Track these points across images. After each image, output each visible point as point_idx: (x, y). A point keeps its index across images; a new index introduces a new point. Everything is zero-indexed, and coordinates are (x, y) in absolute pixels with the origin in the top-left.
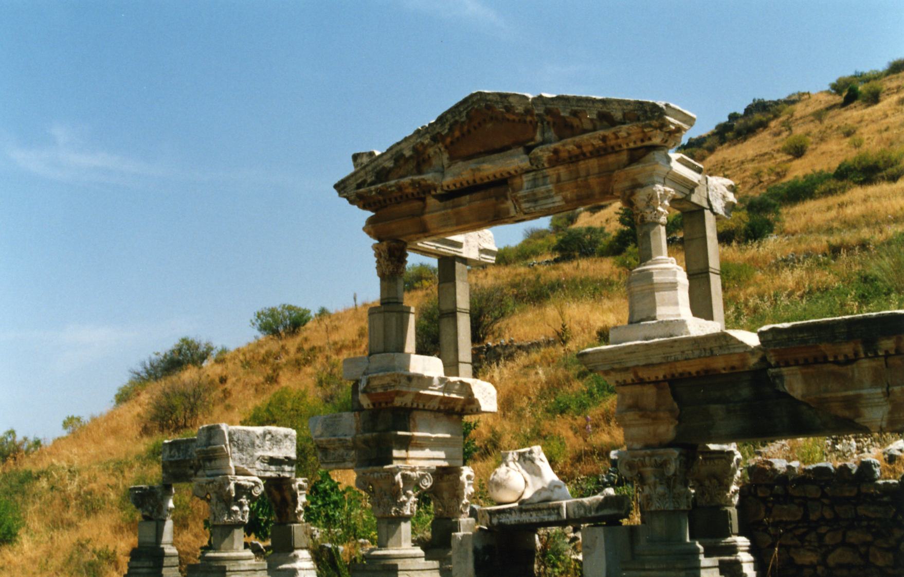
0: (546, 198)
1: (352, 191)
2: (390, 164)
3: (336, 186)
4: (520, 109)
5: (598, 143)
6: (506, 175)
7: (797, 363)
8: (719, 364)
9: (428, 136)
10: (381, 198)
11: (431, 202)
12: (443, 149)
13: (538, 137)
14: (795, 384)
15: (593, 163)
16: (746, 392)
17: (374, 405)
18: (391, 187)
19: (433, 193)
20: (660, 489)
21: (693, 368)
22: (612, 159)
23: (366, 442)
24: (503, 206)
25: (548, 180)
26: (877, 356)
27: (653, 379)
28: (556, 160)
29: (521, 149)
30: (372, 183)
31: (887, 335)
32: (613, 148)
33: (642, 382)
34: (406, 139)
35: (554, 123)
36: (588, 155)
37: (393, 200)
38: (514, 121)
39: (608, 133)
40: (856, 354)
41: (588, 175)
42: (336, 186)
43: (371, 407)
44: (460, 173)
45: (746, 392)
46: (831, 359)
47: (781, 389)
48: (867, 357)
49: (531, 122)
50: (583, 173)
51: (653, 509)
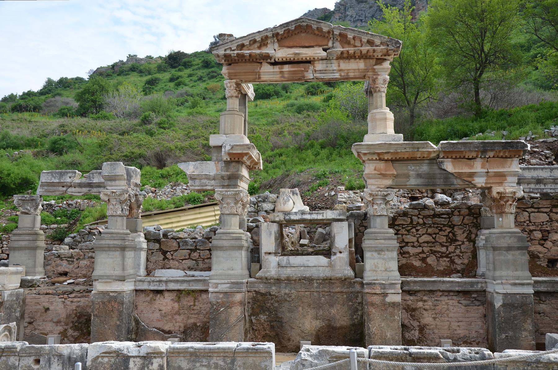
0: (331, 73)
2: (246, 43)
5: (364, 52)
7: (452, 158)
10: (236, 58)
12: (276, 41)
13: (330, 44)
14: (449, 166)
16: (425, 168)
17: (231, 159)
19: (269, 61)
20: (383, 206)
23: (222, 177)
25: (333, 65)
26: (485, 157)
27: (386, 158)
29: (321, 48)
30: (234, 50)
33: (380, 160)
34: (259, 32)
36: (357, 57)
37: (244, 60)
40: (477, 156)
43: (229, 159)
44: (282, 53)
46: (467, 157)
47: (443, 168)
48: (481, 157)
51: (379, 214)
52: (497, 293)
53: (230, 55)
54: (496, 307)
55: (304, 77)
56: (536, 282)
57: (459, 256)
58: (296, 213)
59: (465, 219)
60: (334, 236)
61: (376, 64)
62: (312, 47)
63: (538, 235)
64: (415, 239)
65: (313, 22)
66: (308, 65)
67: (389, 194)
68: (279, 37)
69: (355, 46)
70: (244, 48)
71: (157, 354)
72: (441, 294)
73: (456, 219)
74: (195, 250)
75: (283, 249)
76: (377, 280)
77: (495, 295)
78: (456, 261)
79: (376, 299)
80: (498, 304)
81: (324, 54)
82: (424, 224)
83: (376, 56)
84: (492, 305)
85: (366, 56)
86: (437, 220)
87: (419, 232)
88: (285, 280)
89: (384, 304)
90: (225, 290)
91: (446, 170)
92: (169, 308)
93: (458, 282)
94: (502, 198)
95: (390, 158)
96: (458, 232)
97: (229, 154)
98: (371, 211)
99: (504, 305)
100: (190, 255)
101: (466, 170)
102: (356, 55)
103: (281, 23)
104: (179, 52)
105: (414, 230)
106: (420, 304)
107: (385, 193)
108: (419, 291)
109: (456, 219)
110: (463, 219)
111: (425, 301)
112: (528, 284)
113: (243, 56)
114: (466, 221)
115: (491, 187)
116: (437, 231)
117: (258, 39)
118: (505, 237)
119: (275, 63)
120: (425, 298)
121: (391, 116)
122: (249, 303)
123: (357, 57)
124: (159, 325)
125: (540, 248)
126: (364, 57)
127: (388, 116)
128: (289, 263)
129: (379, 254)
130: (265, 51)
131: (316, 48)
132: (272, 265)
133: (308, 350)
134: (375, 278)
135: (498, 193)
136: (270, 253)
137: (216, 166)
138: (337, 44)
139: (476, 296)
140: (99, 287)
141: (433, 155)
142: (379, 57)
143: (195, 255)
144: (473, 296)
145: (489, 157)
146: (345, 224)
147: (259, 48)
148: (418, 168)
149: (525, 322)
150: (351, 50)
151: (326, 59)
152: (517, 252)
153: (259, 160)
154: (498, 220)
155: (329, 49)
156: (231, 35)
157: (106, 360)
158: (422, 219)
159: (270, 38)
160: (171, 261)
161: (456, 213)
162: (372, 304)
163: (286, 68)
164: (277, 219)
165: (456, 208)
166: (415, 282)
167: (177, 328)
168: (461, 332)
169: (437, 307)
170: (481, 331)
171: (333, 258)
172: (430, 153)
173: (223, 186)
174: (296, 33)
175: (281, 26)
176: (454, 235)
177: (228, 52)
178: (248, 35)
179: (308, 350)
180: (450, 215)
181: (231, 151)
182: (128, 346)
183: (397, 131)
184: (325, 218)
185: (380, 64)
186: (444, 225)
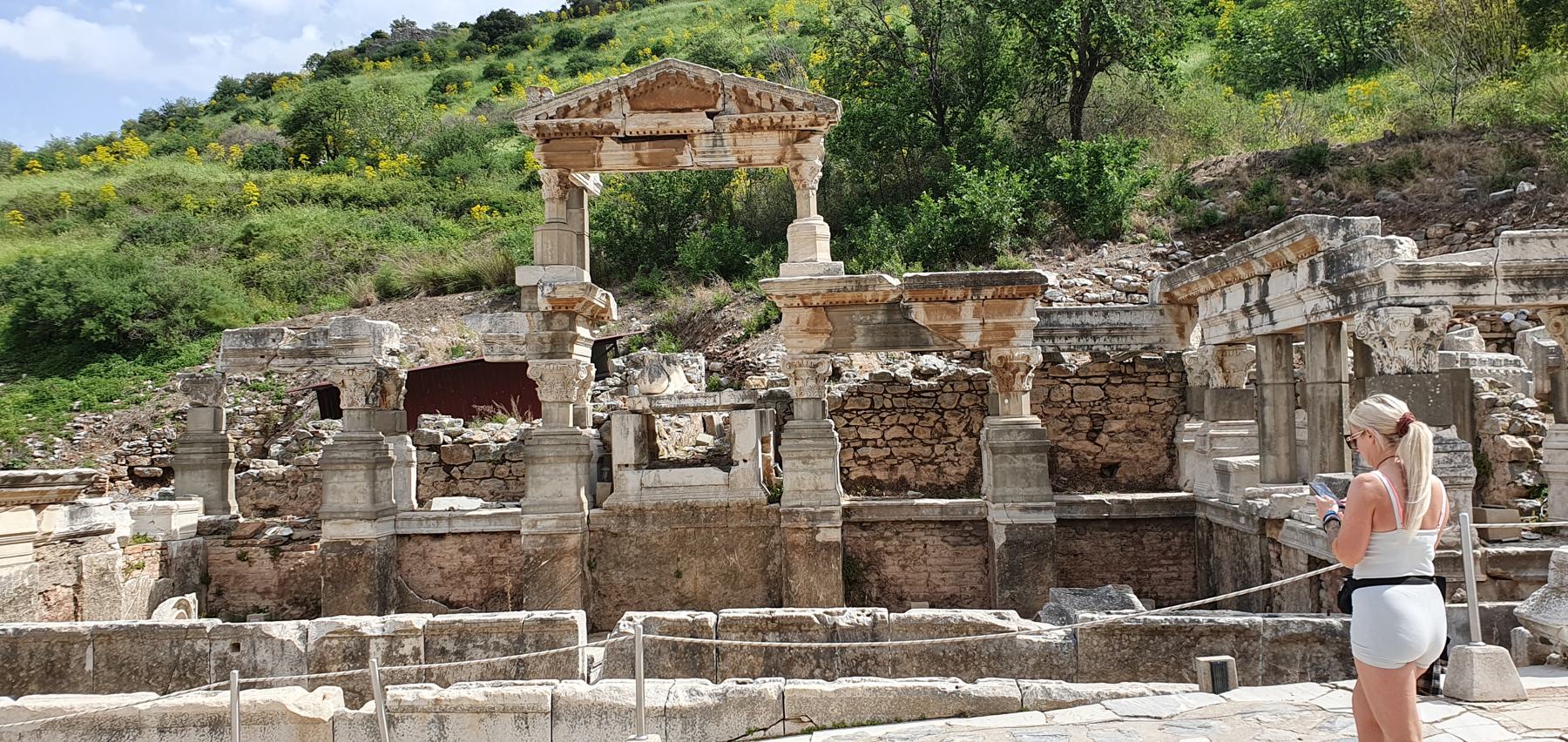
13: (719, 106)
14: (919, 314)
16: (880, 317)
20: (812, 383)
24: (678, 157)
31: (991, 285)
33: (806, 306)
39: (788, 115)
45: (880, 317)
55: (676, 162)
56: (1060, 503)
58: (670, 397)
61: (799, 140)
62: (689, 110)
63: (1085, 423)
64: (878, 435)
69: (762, 110)
71: (410, 631)
73: (947, 400)
74: (503, 461)
75: (650, 456)
78: (947, 470)
79: (801, 538)
80: (999, 539)
81: (709, 124)
82: (894, 408)
84: (992, 544)
86: (914, 401)
87: (886, 422)
89: (813, 543)
90: (549, 531)
92: (456, 563)
93: (942, 506)
94: (1006, 367)
96: (952, 421)
98: (791, 390)
99: (1008, 544)
100: (493, 470)
101: (949, 321)
104: (502, 10)
105: (876, 419)
106: (880, 544)
108: (876, 523)
109: (947, 400)
111: (888, 539)
112: (1047, 508)
113: (569, 127)
114: (964, 402)
116: (915, 420)
119: (626, 140)
120: (887, 534)
121: (824, 229)
122: (591, 550)
124: (439, 592)
125: (1090, 446)
127: (818, 231)
130: (608, 119)
131: (696, 113)
132: (631, 484)
133: (630, 619)
135: (1000, 358)
140: (331, 531)
141: (892, 297)
143: (503, 469)
146: (751, 413)
147: (597, 112)
149: (1040, 569)
152: (1030, 457)
153: (608, 305)
154: (1004, 403)
155: (717, 114)
157: (335, 642)
160: (460, 483)
161: (948, 388)
162: (795, 546)
163: (646, 149)
164: (639, 408)
165: (947, 380)
166: (870, 507)
167: (470, 598)
168: (947, 589)
170: (981, 587)
171: (733, 470)
172: (887, 294)
173: (543, 356)
176: (945, 427)
177: (542, 121)
179: (630, 619)
180: (936, 392)
182: (370, 624)
183: (835, 256)
186: (927, 410)
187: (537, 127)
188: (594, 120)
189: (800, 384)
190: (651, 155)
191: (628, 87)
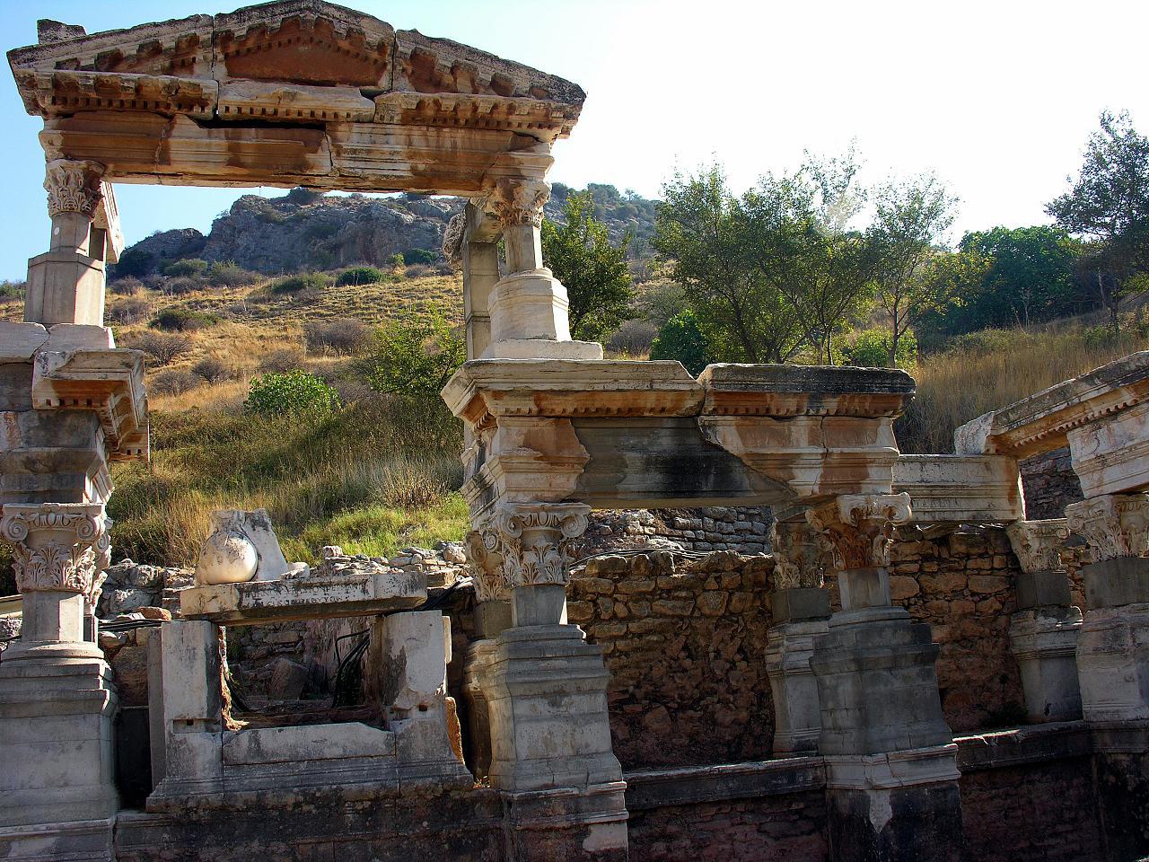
0: (386, 161)
1: (44, 69)
2: (129, 49)
3: (13, 56)
4: (373, 37)
6: (330, 118)
8: (650, 401)
9: (210, 30)
11: (185, 127)
12: (221, 57)
13: (384, 83)
15: (461, 135)
16: (665, 442)
17: (62, 402)
18: (128, 80)
21: (616, 403)
22: (491, 137)
23: (30, 463)
24: (310, 157)
25: (392, 139)
27: (558, 411)
28: (412, 118)
32: (499, 123)
33: (541, 414)
34: (172, 23)
35: (413, 72)
36: (462, 122)
37: (116, 104)
38: (348, 52)
40: (798, 411)
41: (454, 146)
42: (13, 56)
43: (55, 403)
46: (774, 412)
48: (807, 415)
49: (376, 61)
50: (448, 144)
52: (876, 788)
53: (73, 85)
54: (878, 830)
57: (725, 703)
59: (735, 599)
60: (402, 658)
65: (337, 14)
66: (314, 134)
67: (571, 519)
68: (232, 48)
70: (123, 66)
72: (713, 810)
76: (553, 786)
77: (872, 795)
78: (719, 716)
81: (366, 106)
83: (515, 124)
85: (487, 123)
88: (248, 809)
91: (721, 449)
95: (570, 409)
97: (58, 383)
101: (773, 449)
102: (460, 115)
103: (242, 6)
107: (559, 516)
110: (729, 601)
115: (834, 496)
117: (167, 42)
118: (882, 629)
119: (214, 123)
121: (560, 291)
123: (462, 122)
126: (482, 124)
128: (259, 751)
129: (553, 704)
131: (339, 88)
134: (547, 780)
135: (854, 511)
136: (190, 722)
137: (11, 428)
138: (404, 82)
139: (802, 806)
142: (524, 129)
144: (794, 807)
145: (828, 415)
147: (170, 70)
148: (646, 441)
150: (448, 101)
151: (371, 122)
156: (79, 29)
158: (626, 604)
159: (204, 45)
163: (250, 137)
169: (705, 852)
173: (33, 497)
174: (284, 40)
175: (240, 13)
177: (70, 72)
178: (134, 29)
181: (65, 375)
184: (371, 595)
185: (526, 148)
187: (56, 83)
188: (165, 79)
189: (530, 557)
190: (259, 148)
191: (229, 36)
